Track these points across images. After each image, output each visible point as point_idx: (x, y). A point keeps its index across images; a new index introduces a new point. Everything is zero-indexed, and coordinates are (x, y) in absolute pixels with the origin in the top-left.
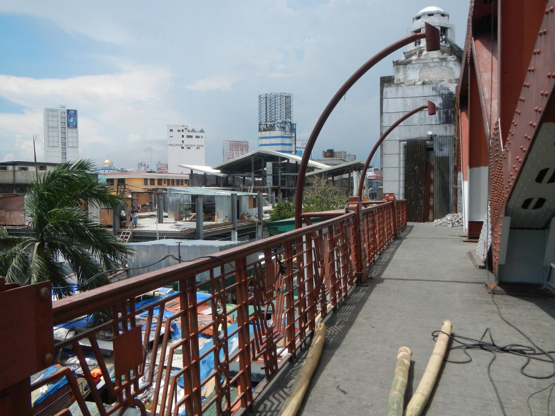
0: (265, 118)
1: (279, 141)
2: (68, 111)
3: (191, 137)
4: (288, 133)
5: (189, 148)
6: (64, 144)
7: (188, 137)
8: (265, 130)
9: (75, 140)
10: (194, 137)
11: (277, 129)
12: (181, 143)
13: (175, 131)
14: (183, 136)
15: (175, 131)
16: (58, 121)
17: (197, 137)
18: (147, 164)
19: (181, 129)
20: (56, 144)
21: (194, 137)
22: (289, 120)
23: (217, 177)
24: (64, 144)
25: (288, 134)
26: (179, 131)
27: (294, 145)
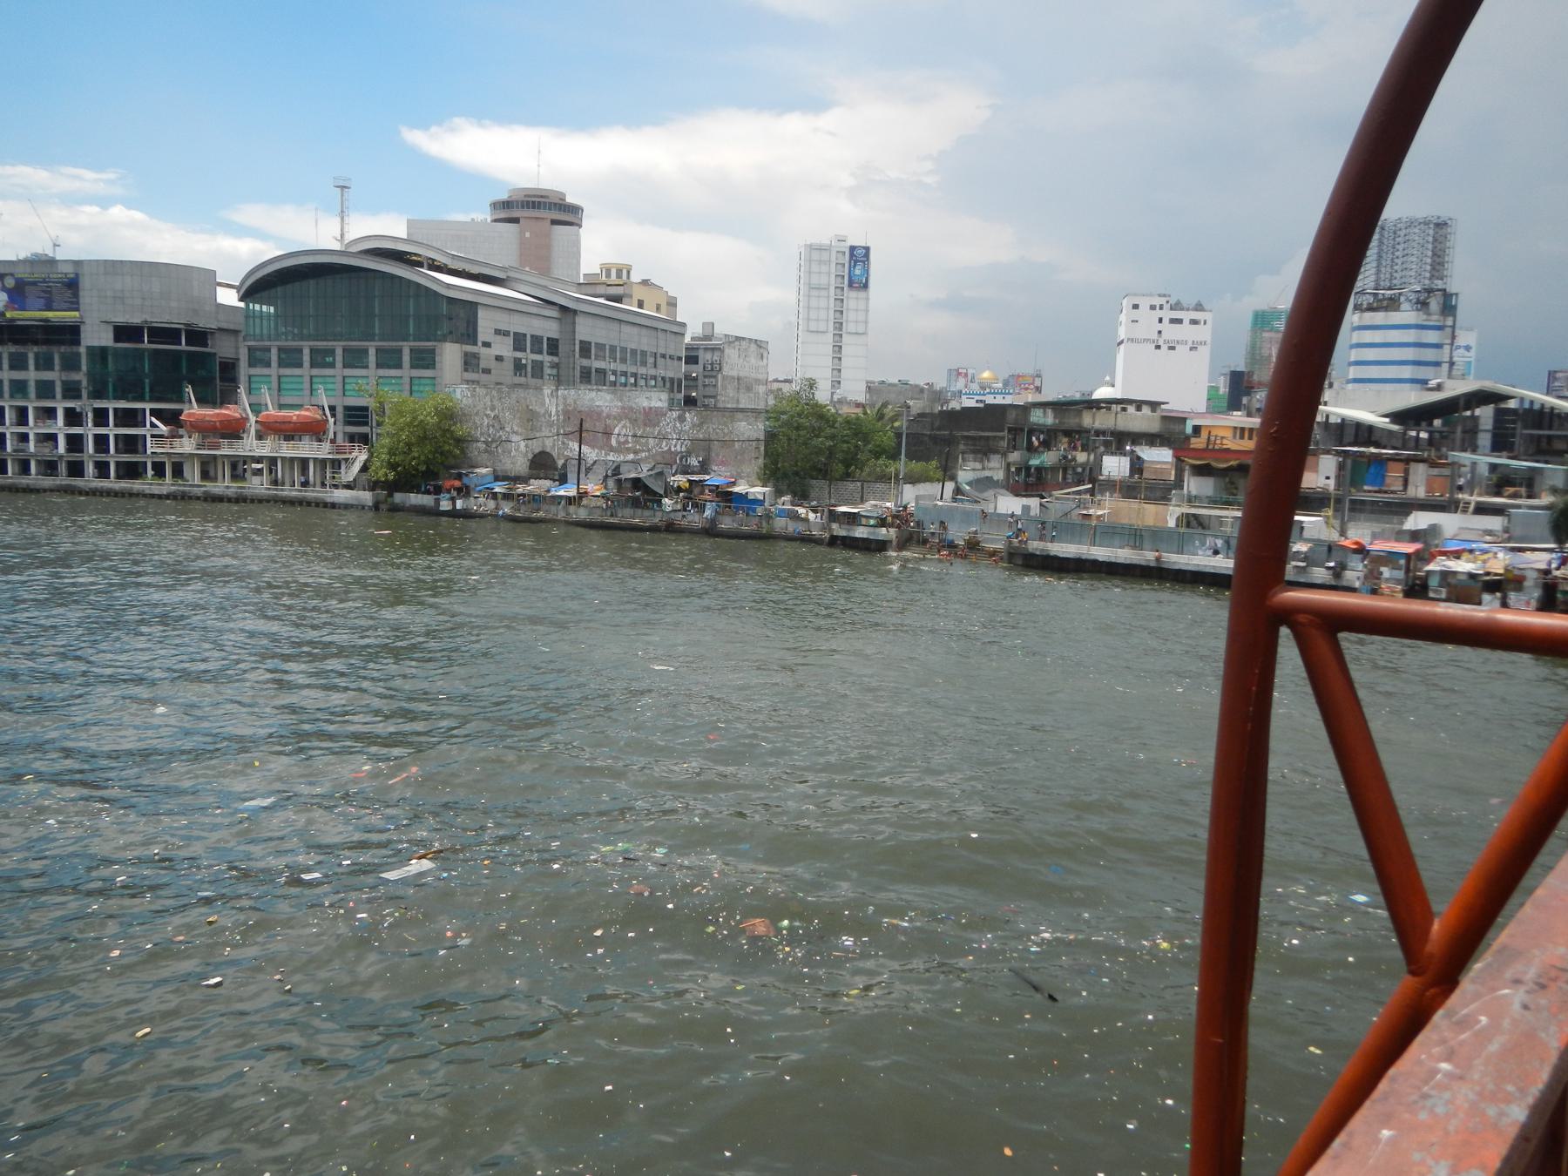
0: (1373, 278)
1: (1410, 336)
2: (853, 248)
3: (1179, 321)
4: (1435, 317)
5: (1172, 348)
6: (839, 325)
7: (1174, 321)
8: (1371, 309)
9: (861, 317)
10: (1186, 322)
11: (1405, 306)
12: (1155, 336)
13: (1144, 304)
14: (1160, 320)
15: (1144, 304)
16: (829, 274)
17: (1194, 322)
18: (970, 372)
19: (1157, 301)
20: (822, 327)
21: (1186, 322)
22: (1439, 284)
23: (1359, 426)
24: (839, 325)
25: (1435, 319)
26: (1153, 308)
27: (1447, 349)
